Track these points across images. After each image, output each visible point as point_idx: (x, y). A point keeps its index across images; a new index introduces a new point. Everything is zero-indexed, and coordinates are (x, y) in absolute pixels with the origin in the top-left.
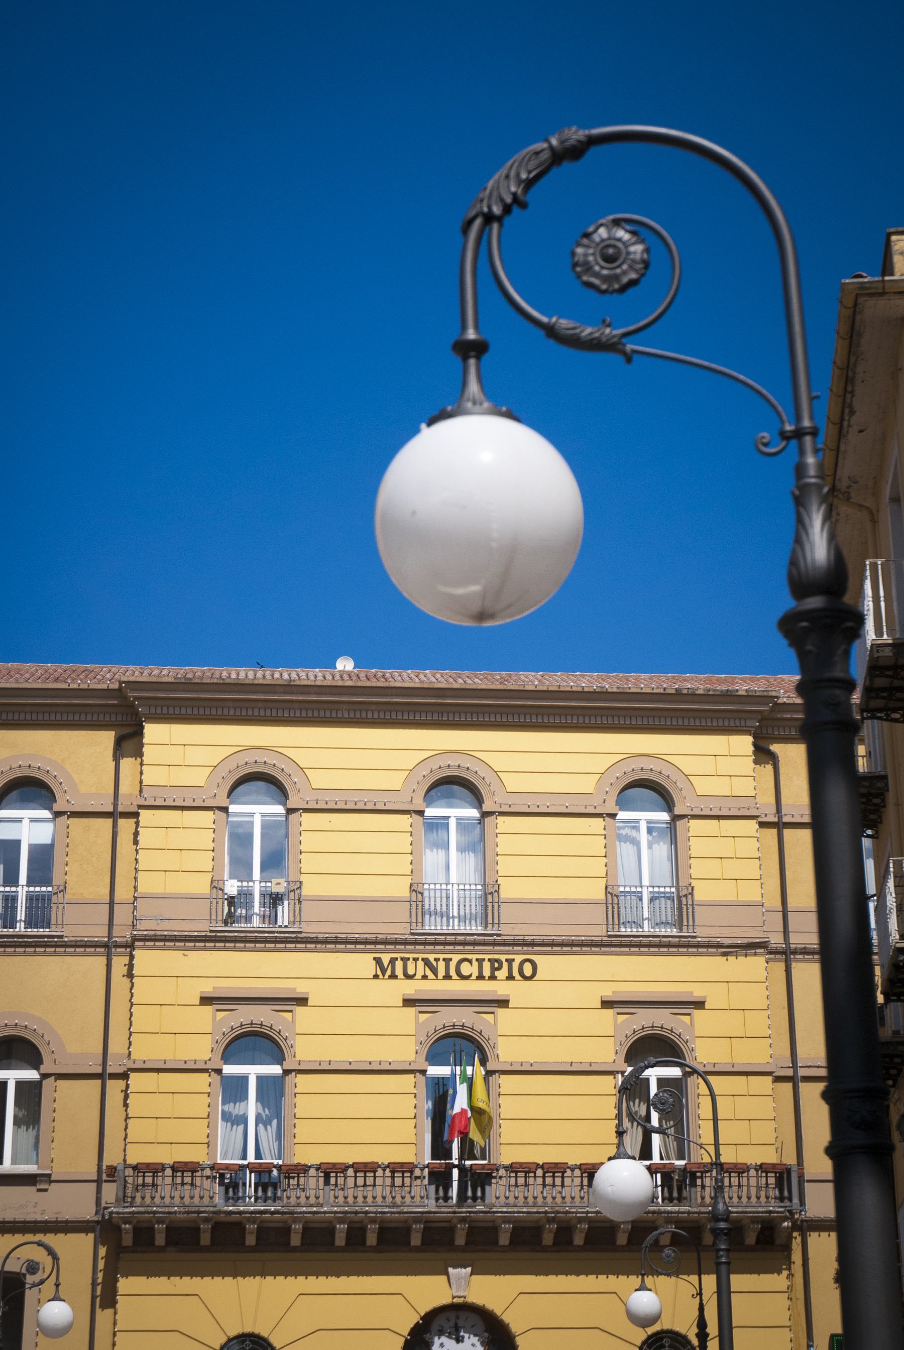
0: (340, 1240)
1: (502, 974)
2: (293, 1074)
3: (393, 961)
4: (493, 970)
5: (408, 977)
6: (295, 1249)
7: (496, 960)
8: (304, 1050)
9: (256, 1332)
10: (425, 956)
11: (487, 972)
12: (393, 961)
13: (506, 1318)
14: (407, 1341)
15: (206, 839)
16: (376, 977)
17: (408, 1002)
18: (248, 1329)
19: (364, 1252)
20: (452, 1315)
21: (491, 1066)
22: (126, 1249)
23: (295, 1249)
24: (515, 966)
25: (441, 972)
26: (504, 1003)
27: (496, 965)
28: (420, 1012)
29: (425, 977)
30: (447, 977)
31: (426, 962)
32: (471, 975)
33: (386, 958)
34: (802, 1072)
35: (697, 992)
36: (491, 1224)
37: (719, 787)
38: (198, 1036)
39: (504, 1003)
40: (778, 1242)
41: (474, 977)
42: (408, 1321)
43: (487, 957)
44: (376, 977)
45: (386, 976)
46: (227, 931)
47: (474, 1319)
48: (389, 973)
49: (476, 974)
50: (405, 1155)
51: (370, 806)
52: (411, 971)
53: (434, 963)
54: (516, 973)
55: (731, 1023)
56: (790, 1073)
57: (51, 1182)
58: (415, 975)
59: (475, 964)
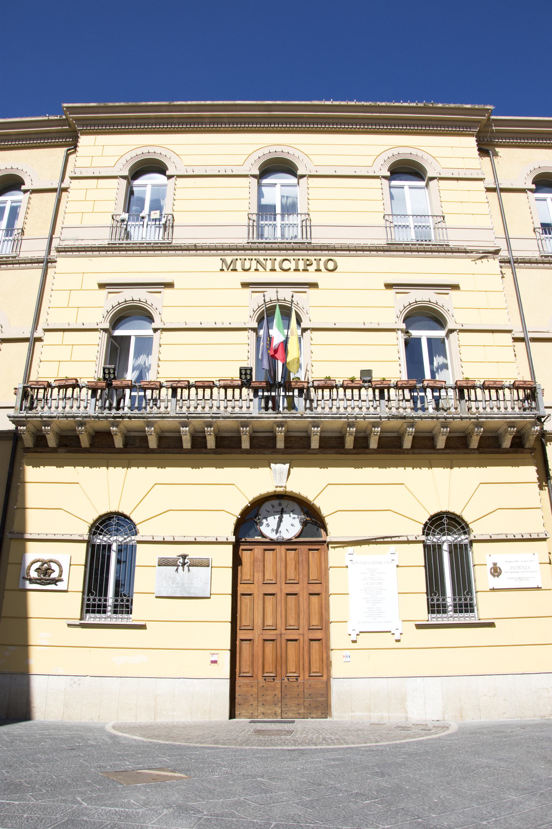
0: (187, 444)
1: (312, 268)
2: (159, 331)
6: (153, 451)
7: (308, 260)
10: (256, 257)
11: (301, 266)
13: (318, 503)
15: (113, 194)
16: (222, 270)
17: (245, 285)
18: (113, 509)
19: (206, 453)
20: (275, 502)
21: (303, 325)
22: (27, 450)
23: (153, 451)
25: (269, 265)
26: (314, 285)
30: (273, 270)
32: (290, 269)
34: (530, 335)
36: (304, 434)
39: (314, 285)
40: (527, 446)
41: (292, 270)
43: (301, 258)
44: (222, 270)
45: (230, 270)
48: (231, 268)
51: (222, 173)
56: (522, 335)
58: (250, 269)
59: (293, 262)
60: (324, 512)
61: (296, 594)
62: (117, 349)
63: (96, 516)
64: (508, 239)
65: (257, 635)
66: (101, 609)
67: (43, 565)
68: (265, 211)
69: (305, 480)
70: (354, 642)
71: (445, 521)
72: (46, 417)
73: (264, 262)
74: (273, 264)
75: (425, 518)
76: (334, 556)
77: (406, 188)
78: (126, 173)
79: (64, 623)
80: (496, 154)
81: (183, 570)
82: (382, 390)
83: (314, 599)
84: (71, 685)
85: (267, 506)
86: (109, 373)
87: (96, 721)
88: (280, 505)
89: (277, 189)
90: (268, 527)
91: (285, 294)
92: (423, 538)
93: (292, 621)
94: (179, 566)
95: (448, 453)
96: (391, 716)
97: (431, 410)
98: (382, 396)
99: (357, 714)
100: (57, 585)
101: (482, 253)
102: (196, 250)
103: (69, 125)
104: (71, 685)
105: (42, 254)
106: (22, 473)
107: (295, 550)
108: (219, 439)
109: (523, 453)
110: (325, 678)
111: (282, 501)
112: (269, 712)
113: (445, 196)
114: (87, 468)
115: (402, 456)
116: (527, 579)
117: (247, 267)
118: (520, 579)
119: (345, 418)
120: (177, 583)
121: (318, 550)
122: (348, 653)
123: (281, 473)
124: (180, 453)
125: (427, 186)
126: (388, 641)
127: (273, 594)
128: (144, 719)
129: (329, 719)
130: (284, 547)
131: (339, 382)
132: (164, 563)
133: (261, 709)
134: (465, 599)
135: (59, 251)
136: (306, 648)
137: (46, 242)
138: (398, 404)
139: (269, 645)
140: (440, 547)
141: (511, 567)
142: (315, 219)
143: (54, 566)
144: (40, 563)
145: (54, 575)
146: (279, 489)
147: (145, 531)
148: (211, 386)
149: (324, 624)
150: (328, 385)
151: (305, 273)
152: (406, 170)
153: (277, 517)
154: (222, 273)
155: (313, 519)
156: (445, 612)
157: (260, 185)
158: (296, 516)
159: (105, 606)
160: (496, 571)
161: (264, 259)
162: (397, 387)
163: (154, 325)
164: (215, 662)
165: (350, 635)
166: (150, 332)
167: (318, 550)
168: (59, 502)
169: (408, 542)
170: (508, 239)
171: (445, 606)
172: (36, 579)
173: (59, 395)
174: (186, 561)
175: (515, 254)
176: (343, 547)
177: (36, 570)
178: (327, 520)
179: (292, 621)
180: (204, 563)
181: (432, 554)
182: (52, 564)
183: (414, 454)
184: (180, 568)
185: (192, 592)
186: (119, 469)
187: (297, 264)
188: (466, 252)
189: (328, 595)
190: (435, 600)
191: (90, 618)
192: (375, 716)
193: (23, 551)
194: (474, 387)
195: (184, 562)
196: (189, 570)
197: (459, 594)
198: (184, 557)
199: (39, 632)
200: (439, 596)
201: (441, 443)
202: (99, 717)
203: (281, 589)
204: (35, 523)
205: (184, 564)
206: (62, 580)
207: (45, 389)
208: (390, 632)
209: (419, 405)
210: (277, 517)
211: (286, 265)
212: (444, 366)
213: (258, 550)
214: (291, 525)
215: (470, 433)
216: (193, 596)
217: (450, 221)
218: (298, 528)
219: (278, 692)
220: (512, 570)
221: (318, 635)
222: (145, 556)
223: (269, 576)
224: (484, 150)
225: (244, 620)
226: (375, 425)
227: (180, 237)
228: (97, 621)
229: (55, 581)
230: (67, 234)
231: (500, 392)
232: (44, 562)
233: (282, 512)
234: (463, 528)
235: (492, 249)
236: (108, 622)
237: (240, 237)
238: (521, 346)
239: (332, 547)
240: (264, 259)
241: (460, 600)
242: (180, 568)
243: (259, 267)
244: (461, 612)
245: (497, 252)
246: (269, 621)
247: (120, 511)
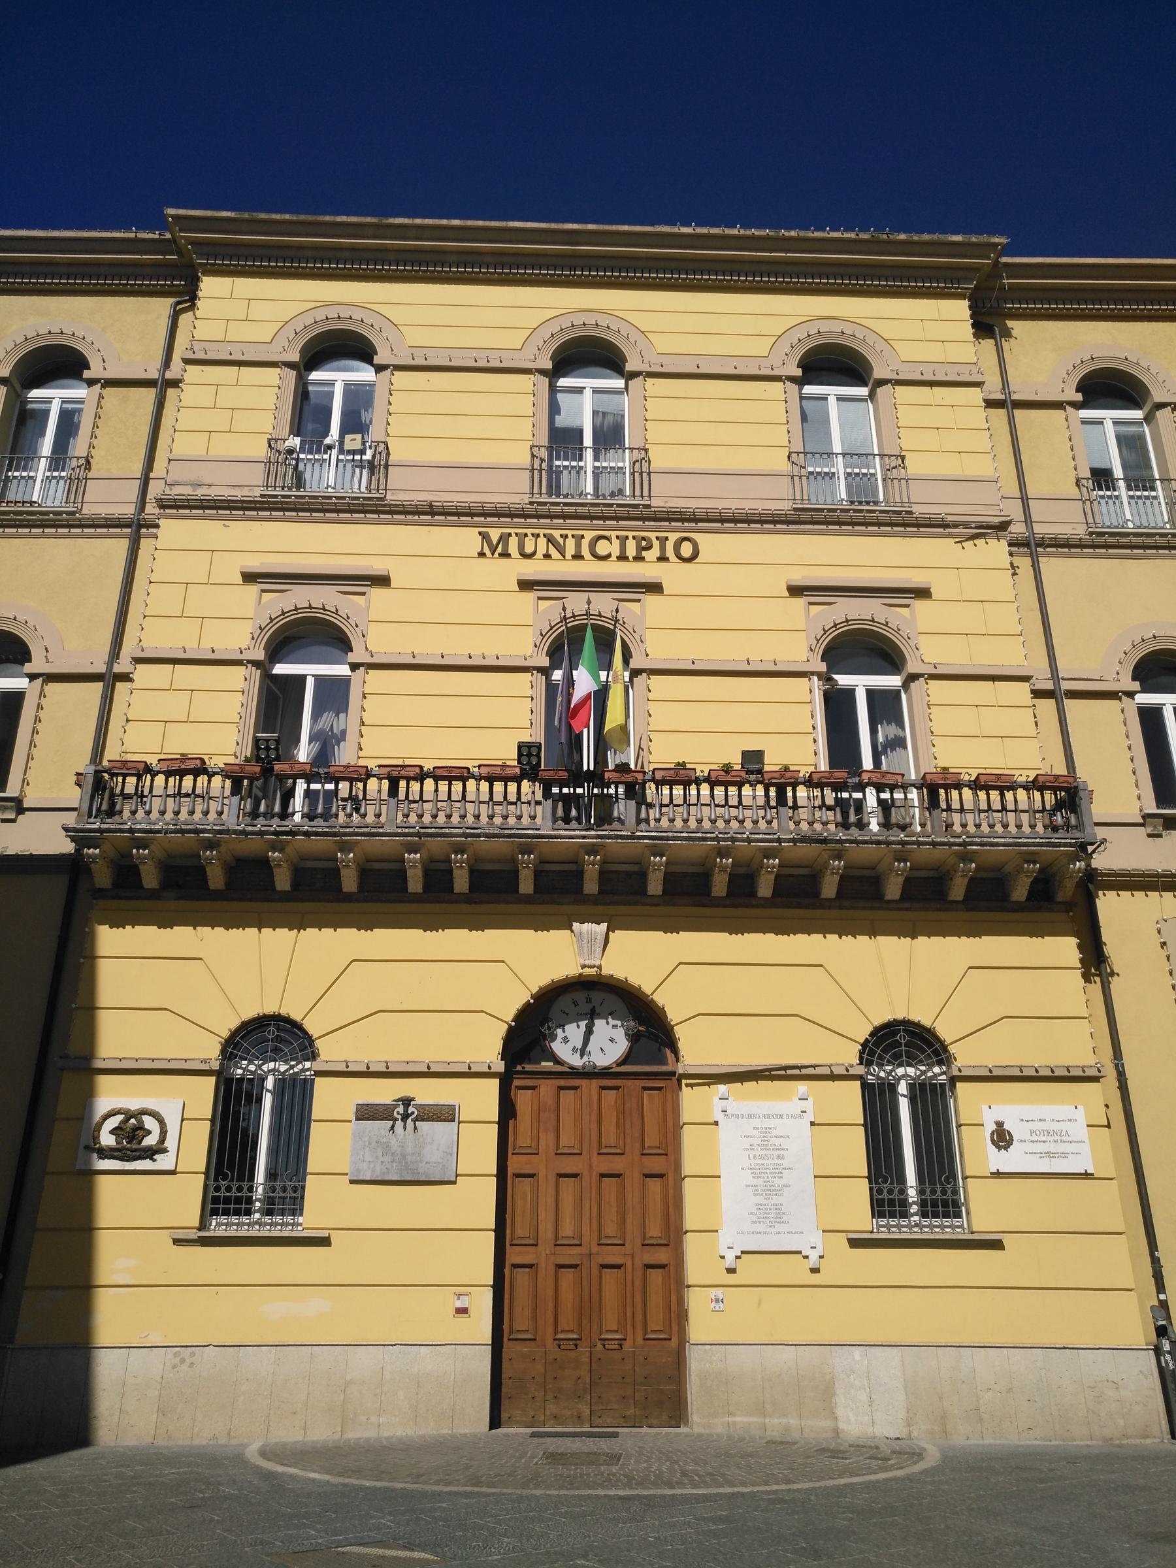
0: (415, 884)
1: (652, 555)
2: (362, 669)
3: (505, 538)
4: (640, 549)
5: (525, 556)
6: (349, 898)
7: (643, 539)
9: (283, 1012)
10: (547, 531)
11: (631, 551)
12: (505, 538)
13: (659, 999)
14: (510, 1028)
15: (269, 398)
16: (482, 554)
17: (526, 585)
18: (270, 1009)
20: (580, 996)
21: (633, 664)
22: (100, 894)
23: (349, 898)
24: (670, 546)
25: (570, 549)
26: (655, 588)
27: (644, 546)
28: (540, 598)
29: (547, 556)
30: (578, 557)
31: (550, 540)
32: (609, 556)
33: (495, 534)
34: (1066, 686)
36: (636, 868)
39: (655, 588)
40: (1060, 898)
41: (614, 558)
42: (512, 1000)
43: (630, 534)
44: (482, 554)
45: (496, 555)
47: (614, 1001)
48: (499, 550)
49: (616, 552)
51: (482, 363)
52: (529, 549)
53: (561, 541)
54: (670, 553)
56: (1049, 686)
57: (21, 810)
58: (534, 553)
59: (616, 543)
60: (673, 1016)
61: (618, 1176)
62: (278, 702)
63: (234, 1023)
64: (1025, 500)
65: (543, 1256)
66: (242, 1206)
67: (126, 1120)
68: (564, 440)
69: (638, 956)
70: (731, 1271)
71: (902, 1037)
72: (140, 831)
73: (561, 541)
74: (578, 546)
75: (863, 1032)
76: (692, 1100)
77: (832, 401)
78: (295, 357)
79: (166, 1237)
80: (1007, 333)
81: (405, 1128)
82: (782, 785)
83: (654, 1185)
84: (174, 1367)
85: (564, 1002)
86: (268, 749)
87: (223, 1441)
88: (589, 1000)
89: (585, 398)
90: (567, 1044)
91: (603, 603)
92: (861, 1070)
93: (610, 1229)
94: (397, 1120)
95: (907, 909)
96: (808, 1427)
97: (874, 827)
98: (781, 799)
99: (738, 1419)
100: (154, 1161)
101: (976, 528)
102: (433, 514)
103: (179, 253)
104: (174, 1367)
105: (129, 510)
106: (89, 939)
107: (617, 1088)
108: (477, 875)
109: (1051, 911)
110: (674, 1343)
111: (590, 995)
112: (567, 1413)
113: (906, 416)
114: (219, 930)
115: (819, 913)
116: (1064, 1155)
117: (529, 549)
118: (1050, 1155)
119: (712, 839)
120: (393, 1154)
121: (660, 1089)
122: (720, 1293)
123: (592, 940)
124: (403, 902)
125: (872, 396)
126: (797, 1271)
127: (575, 1176)
128: (321, 1433)
129: (683, 1429)
130: (595, 1084)
131: (702, 770)
132: (367, 1113)
133: (551, 1408)
134: (944, 1192)
135: (163, 504)
136: (638, 1283)
137: (136, 485)
138: (811, 815)
139: (567, 1276)
140: (893, 1088)
141: (1032, 1132)
142: (659, 459)
143: (149, 1123)
144: (121, 1117)
145: (150, 1141)
146: (587, 971)
147: (330, 1052)
148: (462, 775)
149: (673, 1235)
150: (681, 776)
151: (639, 564)
152: (833, 363)
153: (583, 1024)
154: (482, 560)
156: (905, 1215)
157: (553, 390)
158: (619, 1023)
159: (250, 1201)
160: (1002, 1139)
161: (561, 536)
162: (809, 783)
163: (352, 657)
164: (462, 1311)
165: (723, 1257)
166: (343, 670)
167: (660, 1089)
168: (165, 997)
169: (832, 1077)
170: (1025, 500)
171: (904, 1203)
172: (112, 1149)
173: (166, 788)
174: (411, 1110)
175: (1039, 529)
176: (709, 1084)
177: (111, 1132)
178: (679, 1031)
179: (610, 1229)
180: (445, 1114)
181: (877, 1101)
182: (146, 1118)
183: (840, 908)
184: (399, 1124)
185: (420, 1171)
186: (283, 932)
187: (623, 547)
188: (945, 525)
189: (680, 1179)
190: (885, 1191)
191: (219, 1227)
192: (775, 1425)
193: (89, 1094)
194: (958, 786)
195: (405, 1112)
196: (415, 1128)
197: (932, 1182)
198: (407, 1101)
199: (116, 1259)
200: (892, 1183)
201: (893, 889)
202: (229, 1434)
203: (590, 1166)
204: (115, 1038)
205: (405, 1117)
206: (165, 1151)
207: (139, 777)
208: (800, 1252)
209: (852, 818)
210: (583, 1024)
211: (602, 548)
212: (900, 743)
213: (547, 1088)
214: (609, 1042)
215: (948, 871)
216: (423, 1178)
217: (915, 466)
218: (622, 1045)
219: (584, 1372)
220: (1034, 1138)
221: (661, 1256)
222: (332, 1100)
223: (567, 1139)
224: (985, 325)
225: (519, 1228)
226: (769, 853)
227: (402, 487)
228: (232, 1232)
229: (150, 1153)
230: (178, 472)
231: (1009, 795)
232: (129, 1115)
233: (592, 1015)
234: (936, 1053)
235: (996, 520)
236: (254, 1232)
237: (516, 491)
238: (1048, 706)
239: (687, 1085)
240: (561, 536)
241: (933, 1192)
242: (399, 1124)
243: (553, 551)
244: (936, 1215)
245: (1003, 526)
246: (567, 1229)
247: (283, 1012)
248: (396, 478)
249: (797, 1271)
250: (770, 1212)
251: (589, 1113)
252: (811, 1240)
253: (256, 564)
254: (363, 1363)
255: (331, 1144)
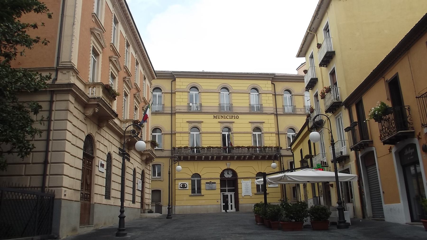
1: (233, 118)
8: (203, 130)
27: (232, 117)
33: (215, 116)
35: (263, 121)
37: (266, 89)
38: (186, 128)
46: (189, 112)
50: (219, 146)
55: (269, 125)
69: (234, 165)
111: (228, 170)
126: (249, 197)
132: (207, 183)
147: (202, 177)
155: (234, 173)
180: (215, 183)
222: (203, 182)
229: (186, 188)
248: (203, 108)
249: (249, 197)
250: (247, 192)
251: (230, 183)
252: (251, 194)
253: (188, 120)
254: (209, 206)
255: (203, 186)
